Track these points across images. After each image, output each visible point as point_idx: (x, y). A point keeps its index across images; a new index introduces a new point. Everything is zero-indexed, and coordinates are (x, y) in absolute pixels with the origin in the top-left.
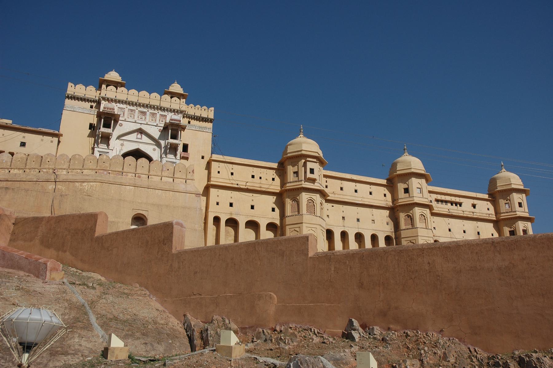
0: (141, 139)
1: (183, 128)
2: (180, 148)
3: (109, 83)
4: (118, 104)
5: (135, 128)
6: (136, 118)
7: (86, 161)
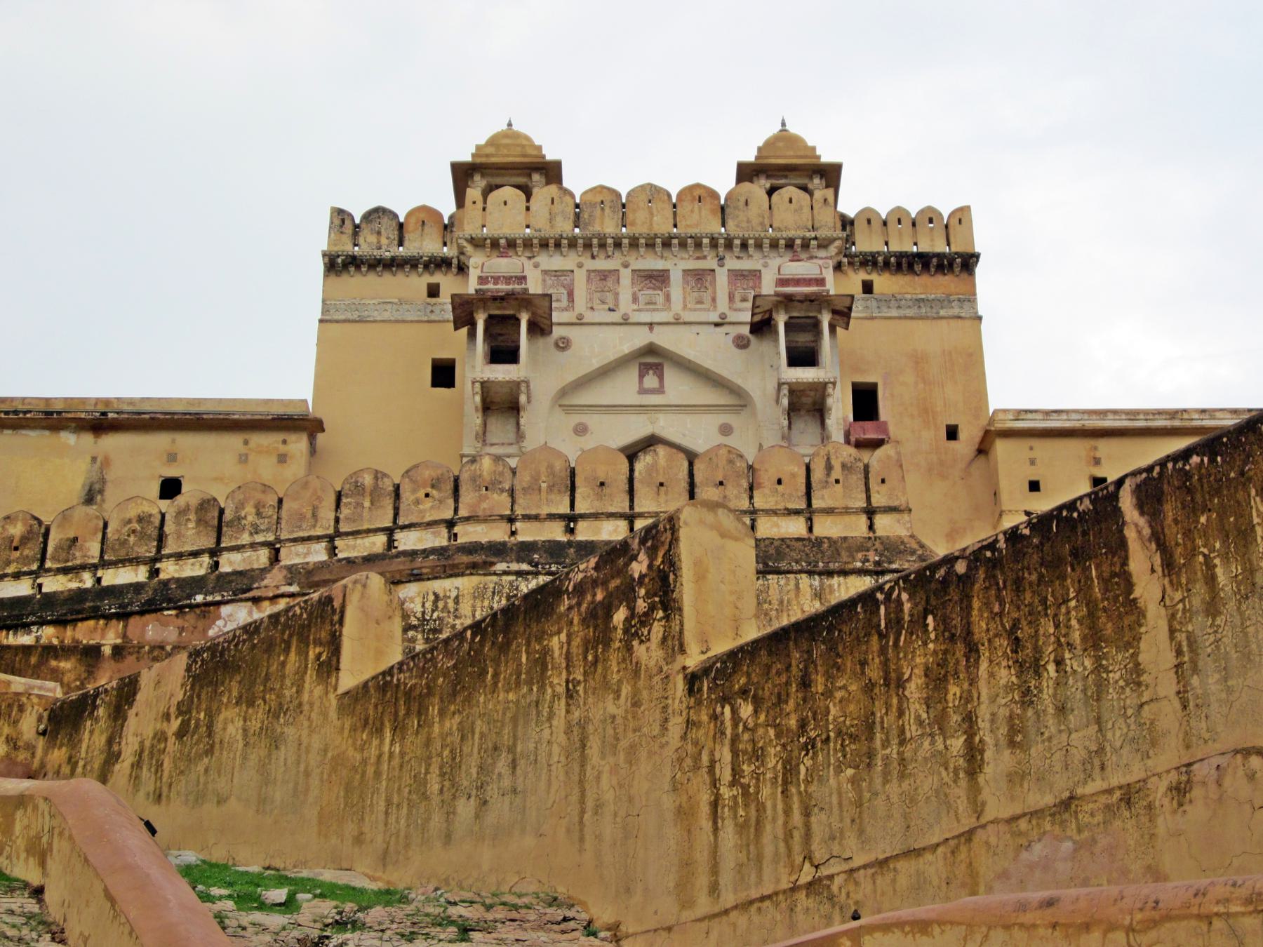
0: (660, 390)
1: (843, 314)
2: (840, 407)
5: (626, 348)
6: (626, 304)
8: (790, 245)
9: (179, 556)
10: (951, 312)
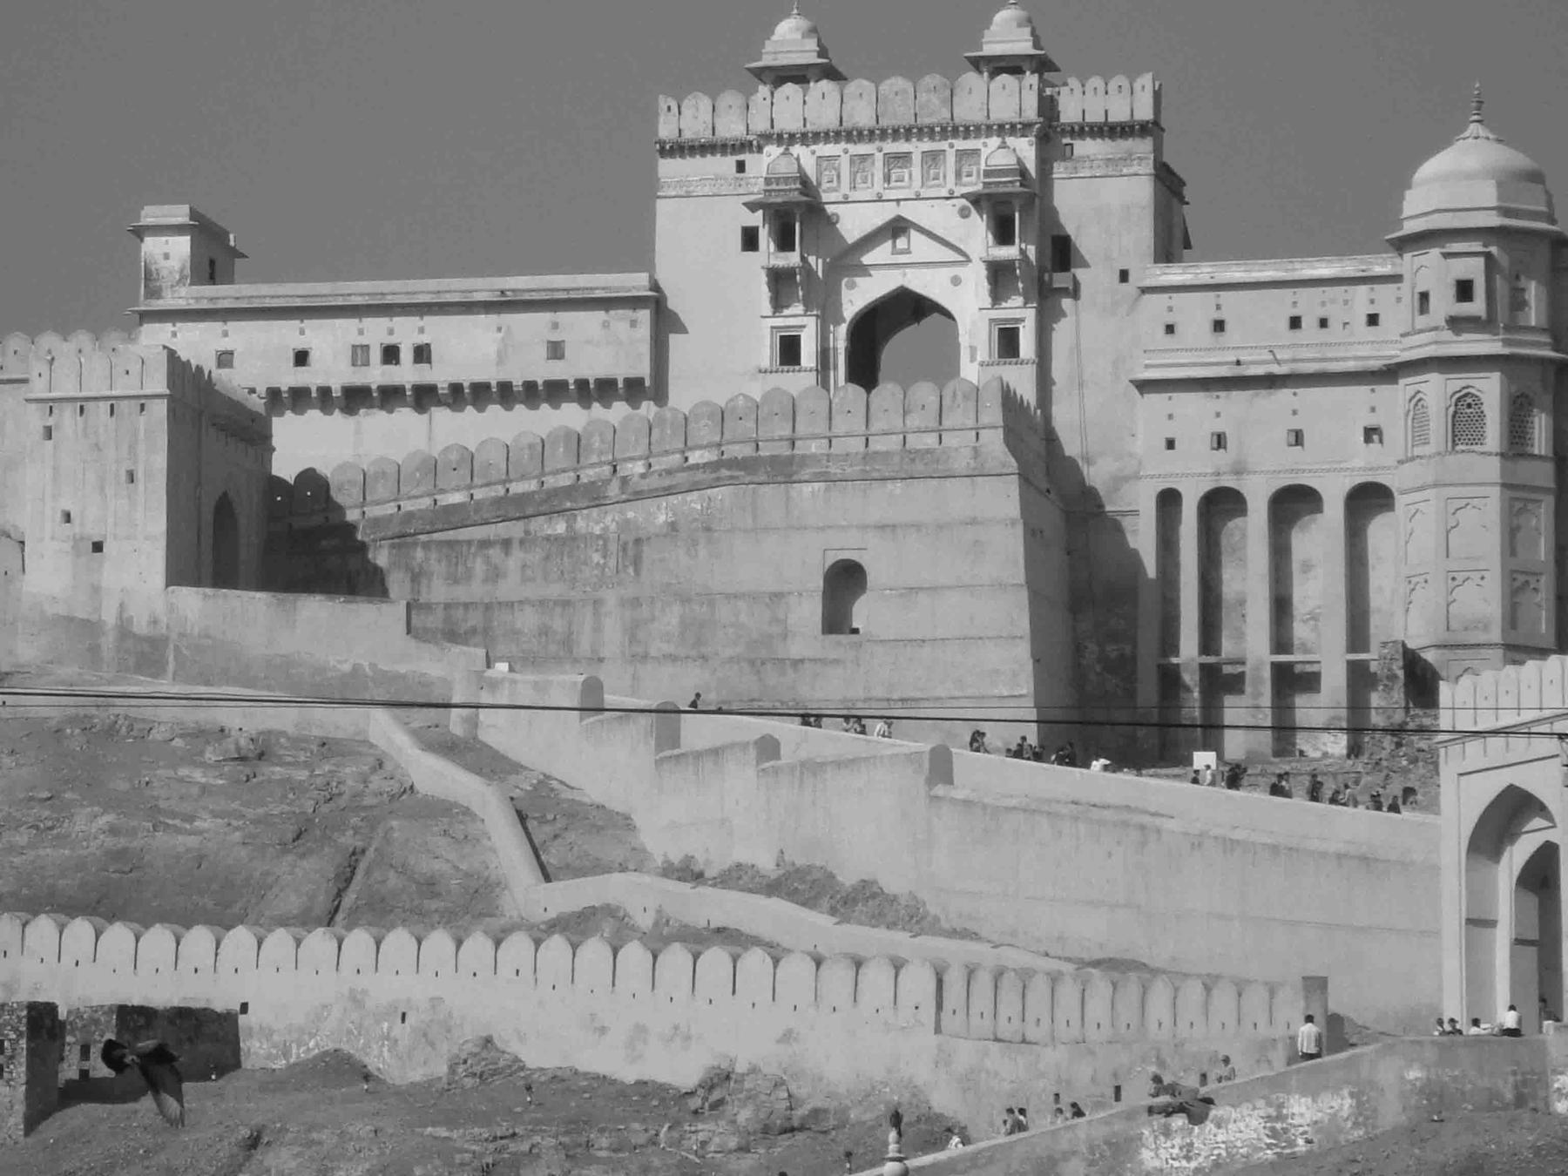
3: (781, 76)
4: (813, 147)
5: (879, 221)
7: (692, 426)
8: (1001, 127)
9: (556, 473)
10: (1132, 170)
